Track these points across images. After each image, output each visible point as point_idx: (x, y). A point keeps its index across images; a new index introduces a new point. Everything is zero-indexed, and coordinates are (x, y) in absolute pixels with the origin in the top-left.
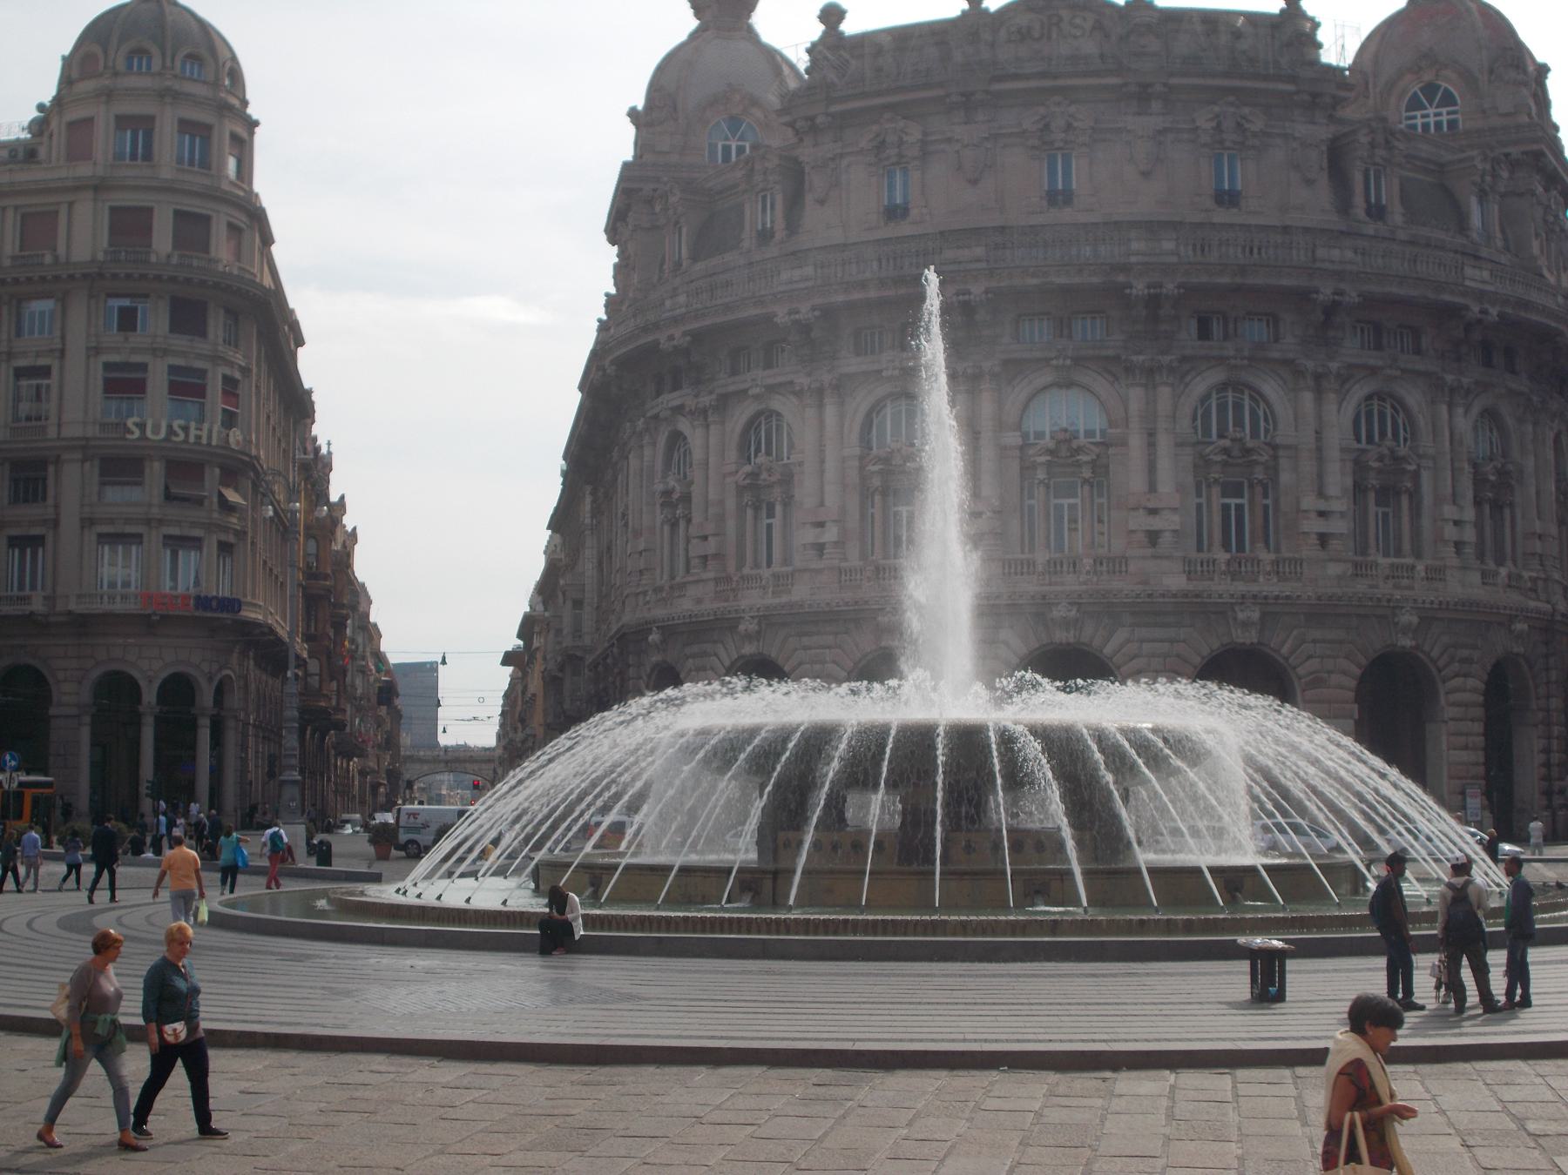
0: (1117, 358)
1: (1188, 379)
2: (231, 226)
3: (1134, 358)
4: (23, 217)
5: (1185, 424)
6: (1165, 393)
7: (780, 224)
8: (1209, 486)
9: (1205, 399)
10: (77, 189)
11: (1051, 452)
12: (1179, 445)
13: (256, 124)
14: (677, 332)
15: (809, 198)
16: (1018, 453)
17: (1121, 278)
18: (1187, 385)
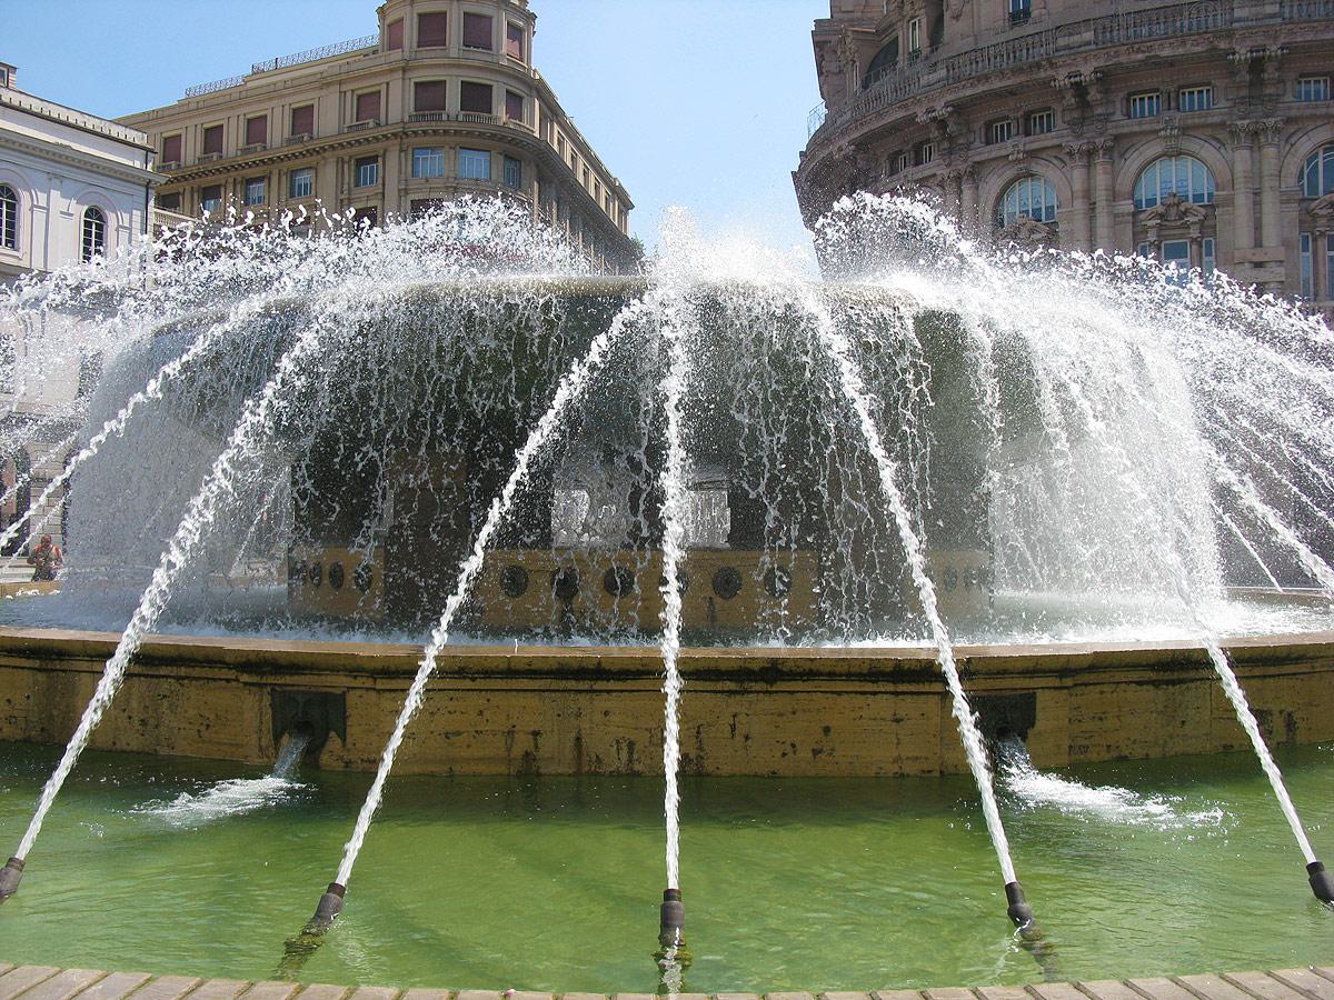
0: (1222, 125)
1: (1293, 140)
2: (507, 91)
3: (1239, 123)
4: (359, 97)
5: (1290, 182)
6: (1270, 152)
7: (926, 42)
8: (1315, 240)
9: (1313, 157)
10: (391, 71)
11: (1161, 216)
12: (1282, 202)
13: (533, 17)
14: (844, 142)
15: (947, 16)
16: (1130, 218)
17: (1223, 45)
18: (1292, 145)
